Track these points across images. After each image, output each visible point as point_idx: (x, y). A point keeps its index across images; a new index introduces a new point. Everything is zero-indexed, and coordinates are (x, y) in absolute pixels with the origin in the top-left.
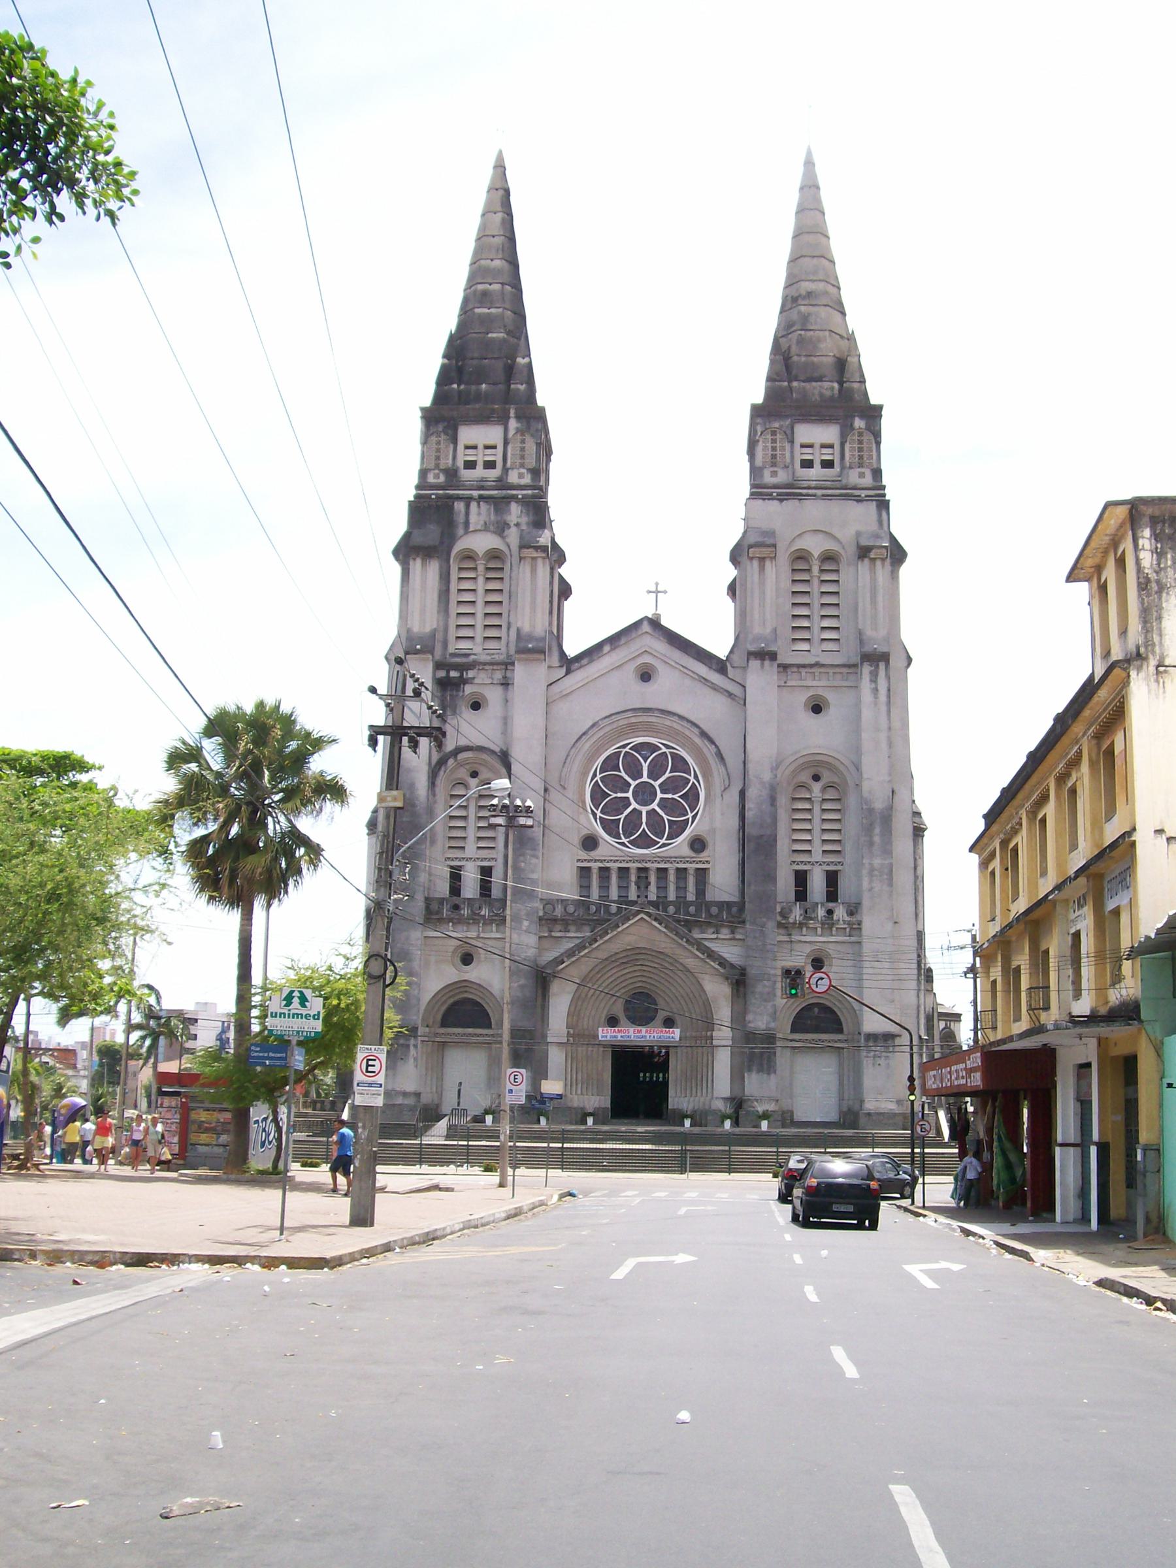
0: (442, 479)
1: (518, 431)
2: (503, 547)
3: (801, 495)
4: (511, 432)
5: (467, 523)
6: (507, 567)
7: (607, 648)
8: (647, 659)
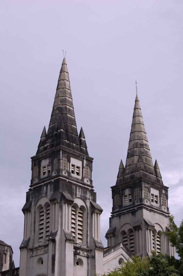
0: (67, 175)
1: (87, 165)
2: (85, 206)
3: (155, 211)
4: (85, 165)
5: (76, 195)
6: (85, 214)
7: (112, 250)
8: (122, 257)
